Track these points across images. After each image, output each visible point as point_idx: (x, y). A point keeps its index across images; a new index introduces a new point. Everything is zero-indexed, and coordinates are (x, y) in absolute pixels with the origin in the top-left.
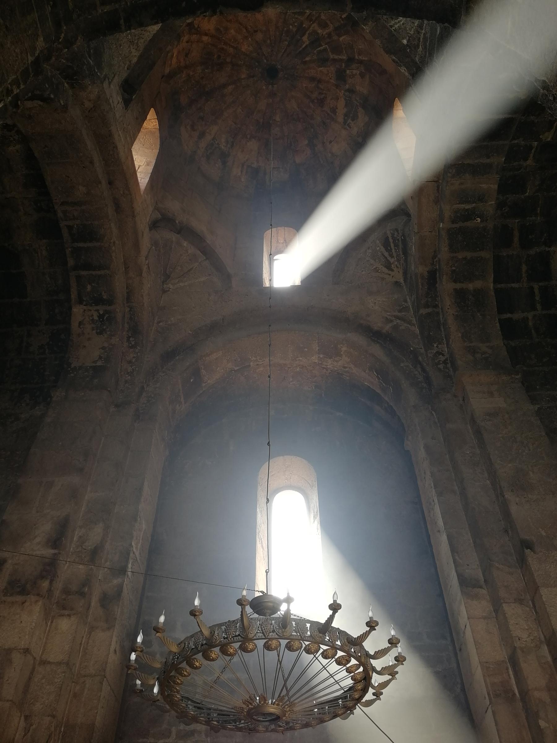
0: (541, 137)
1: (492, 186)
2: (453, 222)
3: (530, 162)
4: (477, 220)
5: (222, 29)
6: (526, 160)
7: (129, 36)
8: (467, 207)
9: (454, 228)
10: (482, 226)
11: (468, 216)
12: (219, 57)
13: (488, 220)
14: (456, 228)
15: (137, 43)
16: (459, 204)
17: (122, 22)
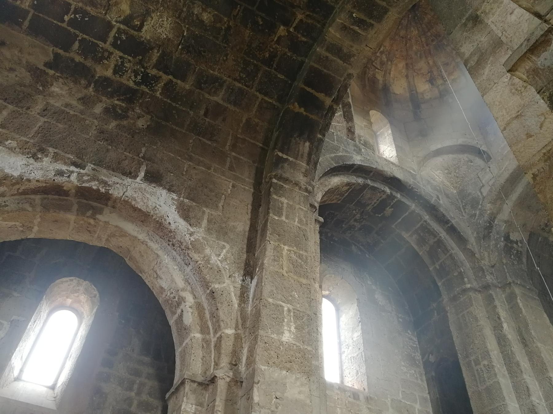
0: (287, 34)
1: (333, 33)
2: (372, 25)
3: (300, 17)
4: (356, 16)
5: (419, 56)
6: (301, 20)
7: (456, 172)
8: (357, 28)
9: (375, 21)
10: (355, 10)
11: (360, 22)
12: (433, 41)
13: (348, 11)
14: (373, 20)
15: (457, 164)
16: (361, 34)
17: (449, 225)
